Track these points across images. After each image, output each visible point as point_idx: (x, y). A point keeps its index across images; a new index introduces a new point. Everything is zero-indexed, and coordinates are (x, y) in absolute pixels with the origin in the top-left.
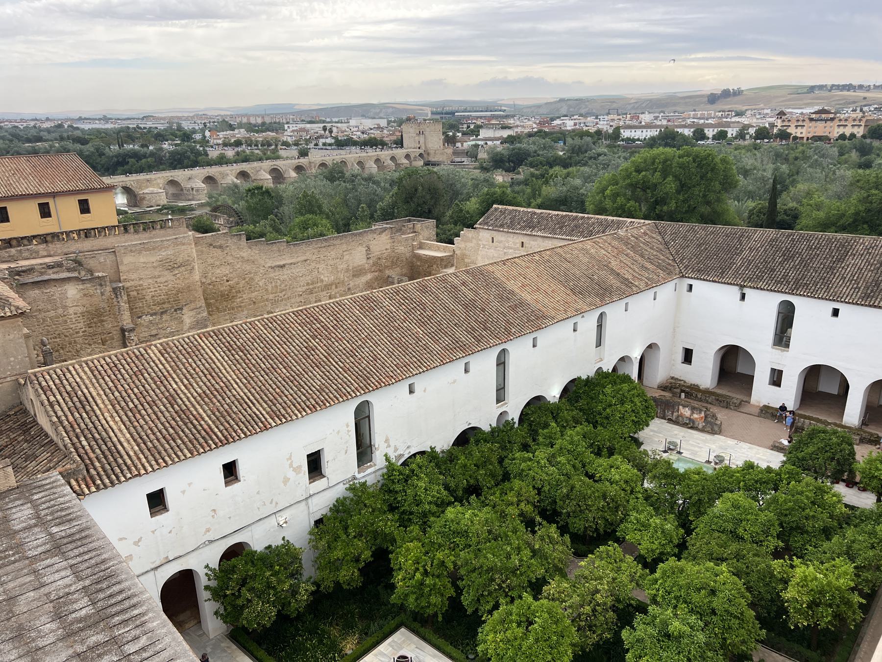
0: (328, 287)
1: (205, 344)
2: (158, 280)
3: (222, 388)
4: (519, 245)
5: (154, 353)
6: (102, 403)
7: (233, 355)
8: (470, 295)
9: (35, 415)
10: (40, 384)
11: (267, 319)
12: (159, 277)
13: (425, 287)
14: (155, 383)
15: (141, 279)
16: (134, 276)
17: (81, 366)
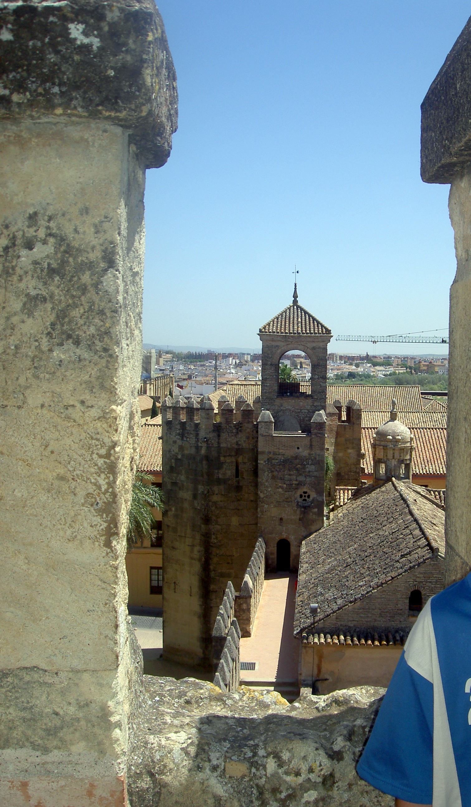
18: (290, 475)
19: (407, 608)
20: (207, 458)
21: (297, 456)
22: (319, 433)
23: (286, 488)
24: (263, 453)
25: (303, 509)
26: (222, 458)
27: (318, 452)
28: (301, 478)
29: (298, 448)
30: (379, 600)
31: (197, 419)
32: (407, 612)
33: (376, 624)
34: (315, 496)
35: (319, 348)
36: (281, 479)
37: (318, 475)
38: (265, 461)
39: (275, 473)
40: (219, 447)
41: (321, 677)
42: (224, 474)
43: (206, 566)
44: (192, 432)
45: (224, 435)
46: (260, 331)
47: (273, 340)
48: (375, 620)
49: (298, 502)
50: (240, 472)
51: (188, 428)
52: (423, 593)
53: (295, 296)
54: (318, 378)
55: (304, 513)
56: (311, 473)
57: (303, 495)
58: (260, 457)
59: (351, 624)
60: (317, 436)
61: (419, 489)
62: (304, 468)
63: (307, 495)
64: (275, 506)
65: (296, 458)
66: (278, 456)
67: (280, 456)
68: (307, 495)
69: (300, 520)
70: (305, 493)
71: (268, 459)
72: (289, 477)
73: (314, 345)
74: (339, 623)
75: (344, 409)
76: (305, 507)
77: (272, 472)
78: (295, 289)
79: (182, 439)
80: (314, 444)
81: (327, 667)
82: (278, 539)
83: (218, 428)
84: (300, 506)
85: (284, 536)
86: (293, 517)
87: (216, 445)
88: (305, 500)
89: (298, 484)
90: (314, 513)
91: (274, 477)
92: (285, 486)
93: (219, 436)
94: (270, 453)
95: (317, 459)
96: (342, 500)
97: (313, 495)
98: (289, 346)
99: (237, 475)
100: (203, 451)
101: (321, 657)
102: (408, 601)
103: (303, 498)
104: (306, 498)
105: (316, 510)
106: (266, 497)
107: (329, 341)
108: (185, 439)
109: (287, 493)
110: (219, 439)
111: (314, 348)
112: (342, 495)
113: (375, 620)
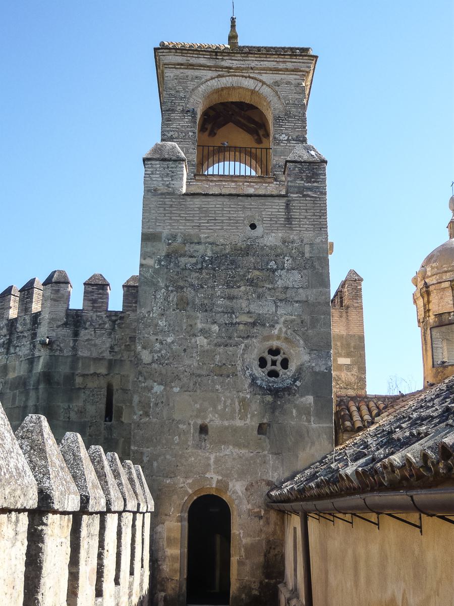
18: (231, 298)
20: (47, 377)
21: (249, 247)
22: (310, 189)
23: (219, 336)
25: (269, 398)
26: (78, 380)
27: (308, 235)
29: (253, 226)
31: (36, 307)
34: (306, 358)
35: (288, 83)
36: (204, 308)
37: (311, 299)
38: (160, 261)
39: (189, 293)
40: (75, 355)
42: (82, 412)
44: (26, 334)
45: (84, 334)
49: (254, 379)
50: (114, 408)
51: (20, 328)
54: (288, 140)
55: (273, 408)
56: (290, 293)
57: (269, 358)
60: (305, 196)
63: (279, 358)
64: (185, 389)
65: (246, 251)
66: (197, 247)
67: (201, 248)
68: (279, 358)
69: (261, 429)
70: (274, 352)
71: (168, 256)
72: (228, 303)
76: (276, 393)
78: (233, 26)
79: (8, 353)
80: (295, 214)
83: (75, 320)
84: (261, 387)
85: (213, 479)
86: (239, 423)
87: (67, 352)
88: (273, 374)
89: (254, 324)
90: (304, 411)
91: (183, 304)
92: (215, 328)
93: (76, 334)
94: (174, 237)
95: (307, 255)
96: (356, 417)
97: (299, 357)
100: (39, 367)
103: (269, 367)
104: (278, 368)
105: (310, 399)
106: (158, 361)
108: (12, 350)
109: (221, 350)
110: (75, 341)
111: (277, 84)
112: (353, 408)
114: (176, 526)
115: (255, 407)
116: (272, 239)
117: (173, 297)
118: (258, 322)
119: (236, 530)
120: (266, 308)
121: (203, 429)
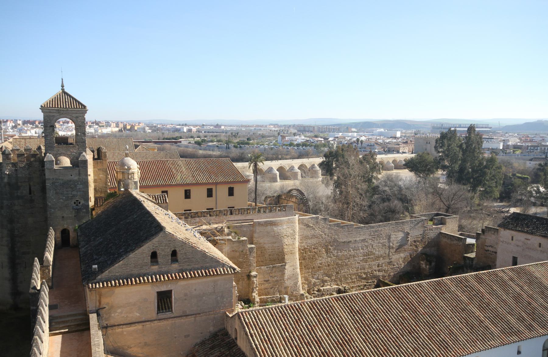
0: (378, 258)
1: (336, 305)
2: (275, 245)
3: (349, 339)
4: (537, 245)
5: (306, 309)
6: (278, 340)
7: (354, 316)
8: (518, 289)
9: (236, 338)
10: (245, 320)
11: (373, 292)
12: (275, 243)
13: (481, 279)
14: (308, 329)
15: (265, 243)
16: (261, 241)
17: (266, 311)
19: (150, 261)
24: (49, 179)
28: (74, 193)
30: (133, 259)
32: (150, 264)
33: (132, 272)
36: (61, 194)
41: (101, 307)
43: (12, 249)
46: (42, 106)
47: (50, 112)
48: (132, 270)
52: (158, 252)
53: (63, 86)
58: (47, 181)
59: (117, 274)
61: (143, 194)
62: (76, 186)
65: (70, 181)
70: (77, 201)
71: (52, 183)
73: (77, 115)
74: (110, 275)
75: (96, 152)
76: (78, 209)
77: (56, 190)
80: (81, 172)
81: (105, 301)
82: (61, 228)
86: (70, 215)
91: (57, 193)
94: (53, 179)
97: (82, 202)
98: (61, 116)
99: (30, 193)
101: (100, 295)
102: (150, 258)
107: (86, 113)
113: (132, 270)
114: (59, 235)
115: (74, 212)
116: (76, 178)
117: (54, 192)
118: (74, 196)
119: (71, 234)
120: (74, 193)
121: (63, 217)
